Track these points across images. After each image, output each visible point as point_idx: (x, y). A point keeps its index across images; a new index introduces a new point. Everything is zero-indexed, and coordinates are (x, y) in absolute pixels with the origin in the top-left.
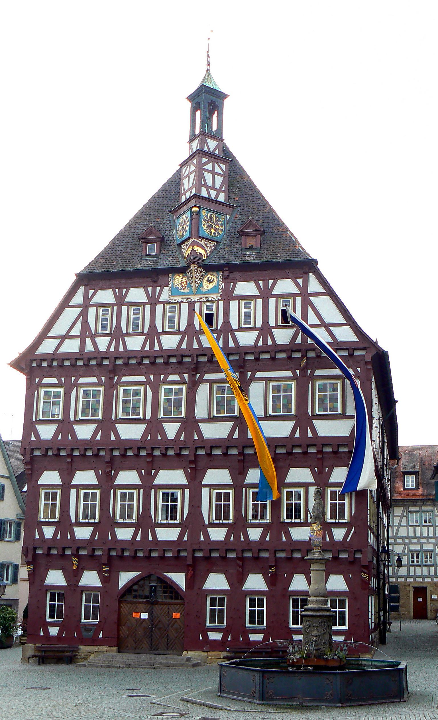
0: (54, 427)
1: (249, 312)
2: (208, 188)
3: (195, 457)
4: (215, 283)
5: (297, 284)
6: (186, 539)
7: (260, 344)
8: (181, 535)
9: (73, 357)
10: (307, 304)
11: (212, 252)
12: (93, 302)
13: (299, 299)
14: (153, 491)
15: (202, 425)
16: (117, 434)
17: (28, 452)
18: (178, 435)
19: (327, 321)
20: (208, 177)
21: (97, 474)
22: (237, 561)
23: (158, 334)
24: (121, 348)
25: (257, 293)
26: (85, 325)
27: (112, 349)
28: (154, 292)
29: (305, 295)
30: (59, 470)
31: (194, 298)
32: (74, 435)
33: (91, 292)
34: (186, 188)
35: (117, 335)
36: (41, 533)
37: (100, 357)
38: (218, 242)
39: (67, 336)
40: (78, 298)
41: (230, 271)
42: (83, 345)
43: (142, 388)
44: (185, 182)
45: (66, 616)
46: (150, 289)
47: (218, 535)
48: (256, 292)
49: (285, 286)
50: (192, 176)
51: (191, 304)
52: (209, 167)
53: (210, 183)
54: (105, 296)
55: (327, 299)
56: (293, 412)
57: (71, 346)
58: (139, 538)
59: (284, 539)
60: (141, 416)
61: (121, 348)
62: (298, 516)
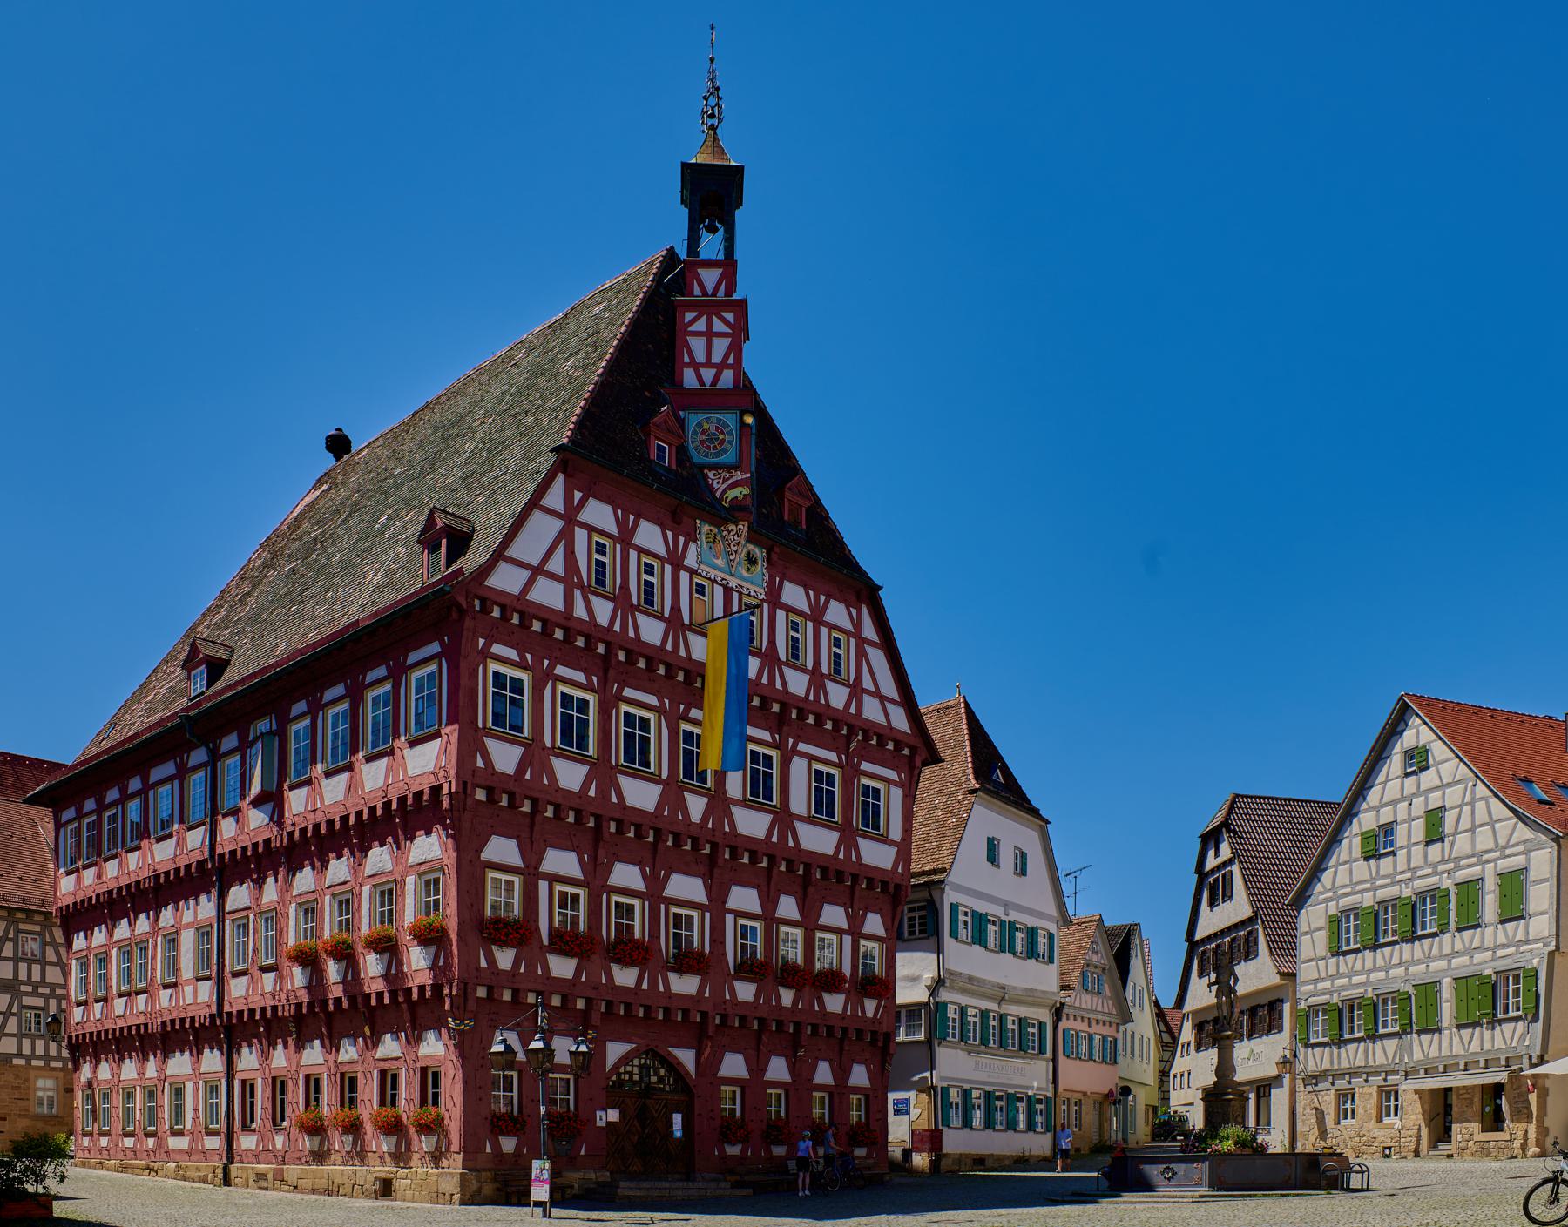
3: (719, 858)
4: (759, 568)
9: (549, 619)
10: (861, 655)
15: (736, 810)
18: (705, 819)
30: (518, 838)
31: (733, 583)
37: (592, 632)
39: (537, 571)
51: (728, 591)
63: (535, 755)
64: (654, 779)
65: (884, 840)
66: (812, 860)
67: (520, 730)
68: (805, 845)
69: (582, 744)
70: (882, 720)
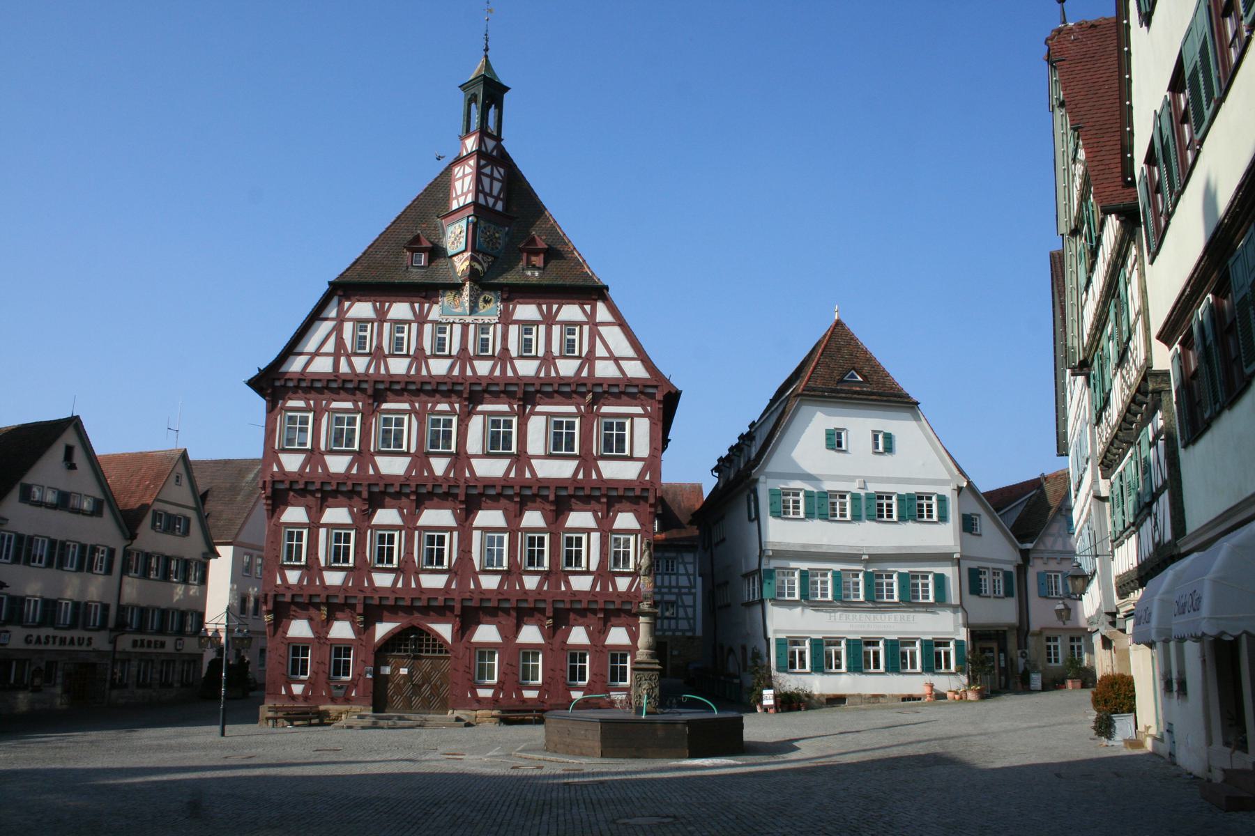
0: (302, 457)
1: (528, 339)
2: (486, 195)
5: (584, 311)
6: (453, 586)
7: (542, 375)
8: (449, 583)
10: (594, 334)
11: (489, 268)
12: (349, 315)
13: (586, 328)
14: (417, 533)
15: (474, 462)
16: (376, 468)
17: (269, 486)
18: (447, 471)
19: (617, 354)
20: (486, 181)
21: (351, 513)
22: (513, 610)
23: (426, 358)
24: (383, 371)
25: (539, 318)
26: (340, 342)
27: (371, 371)
28: (421, 308)
29: (594, 325)
31: (469, 319)
32: (325, 467)
33: (347, 304)
34: (459, 192)
35: (377, 355)
36: (284, 578)
38: (496, 258)
40: (332, 312)
41: (510, 293)
42: (336, 365)
43: (406, 418)
44: (458, 185)
45: (313, 672)
46: (417, 305)
47: (490, 582)
48: (538, 317)
49: (570, 312)
50: (468, 180)
51: (465, 326)
52: (487, 170)
53: (487, 190)
54: (363, 309)
55: (617, 329)
56: (577, 451)
57: (323, 365)
58: (400, 585)
59: (563, 588)
60: (405, 448)
61: (383, 371)
62: (578, 563)
63: (314, 455)
64: (407, 454)
65: (631, 458)
66: (546, 484)
67: (305, 444)
68: (540, 475)
69: (350, 442)
70: (617, 374)
